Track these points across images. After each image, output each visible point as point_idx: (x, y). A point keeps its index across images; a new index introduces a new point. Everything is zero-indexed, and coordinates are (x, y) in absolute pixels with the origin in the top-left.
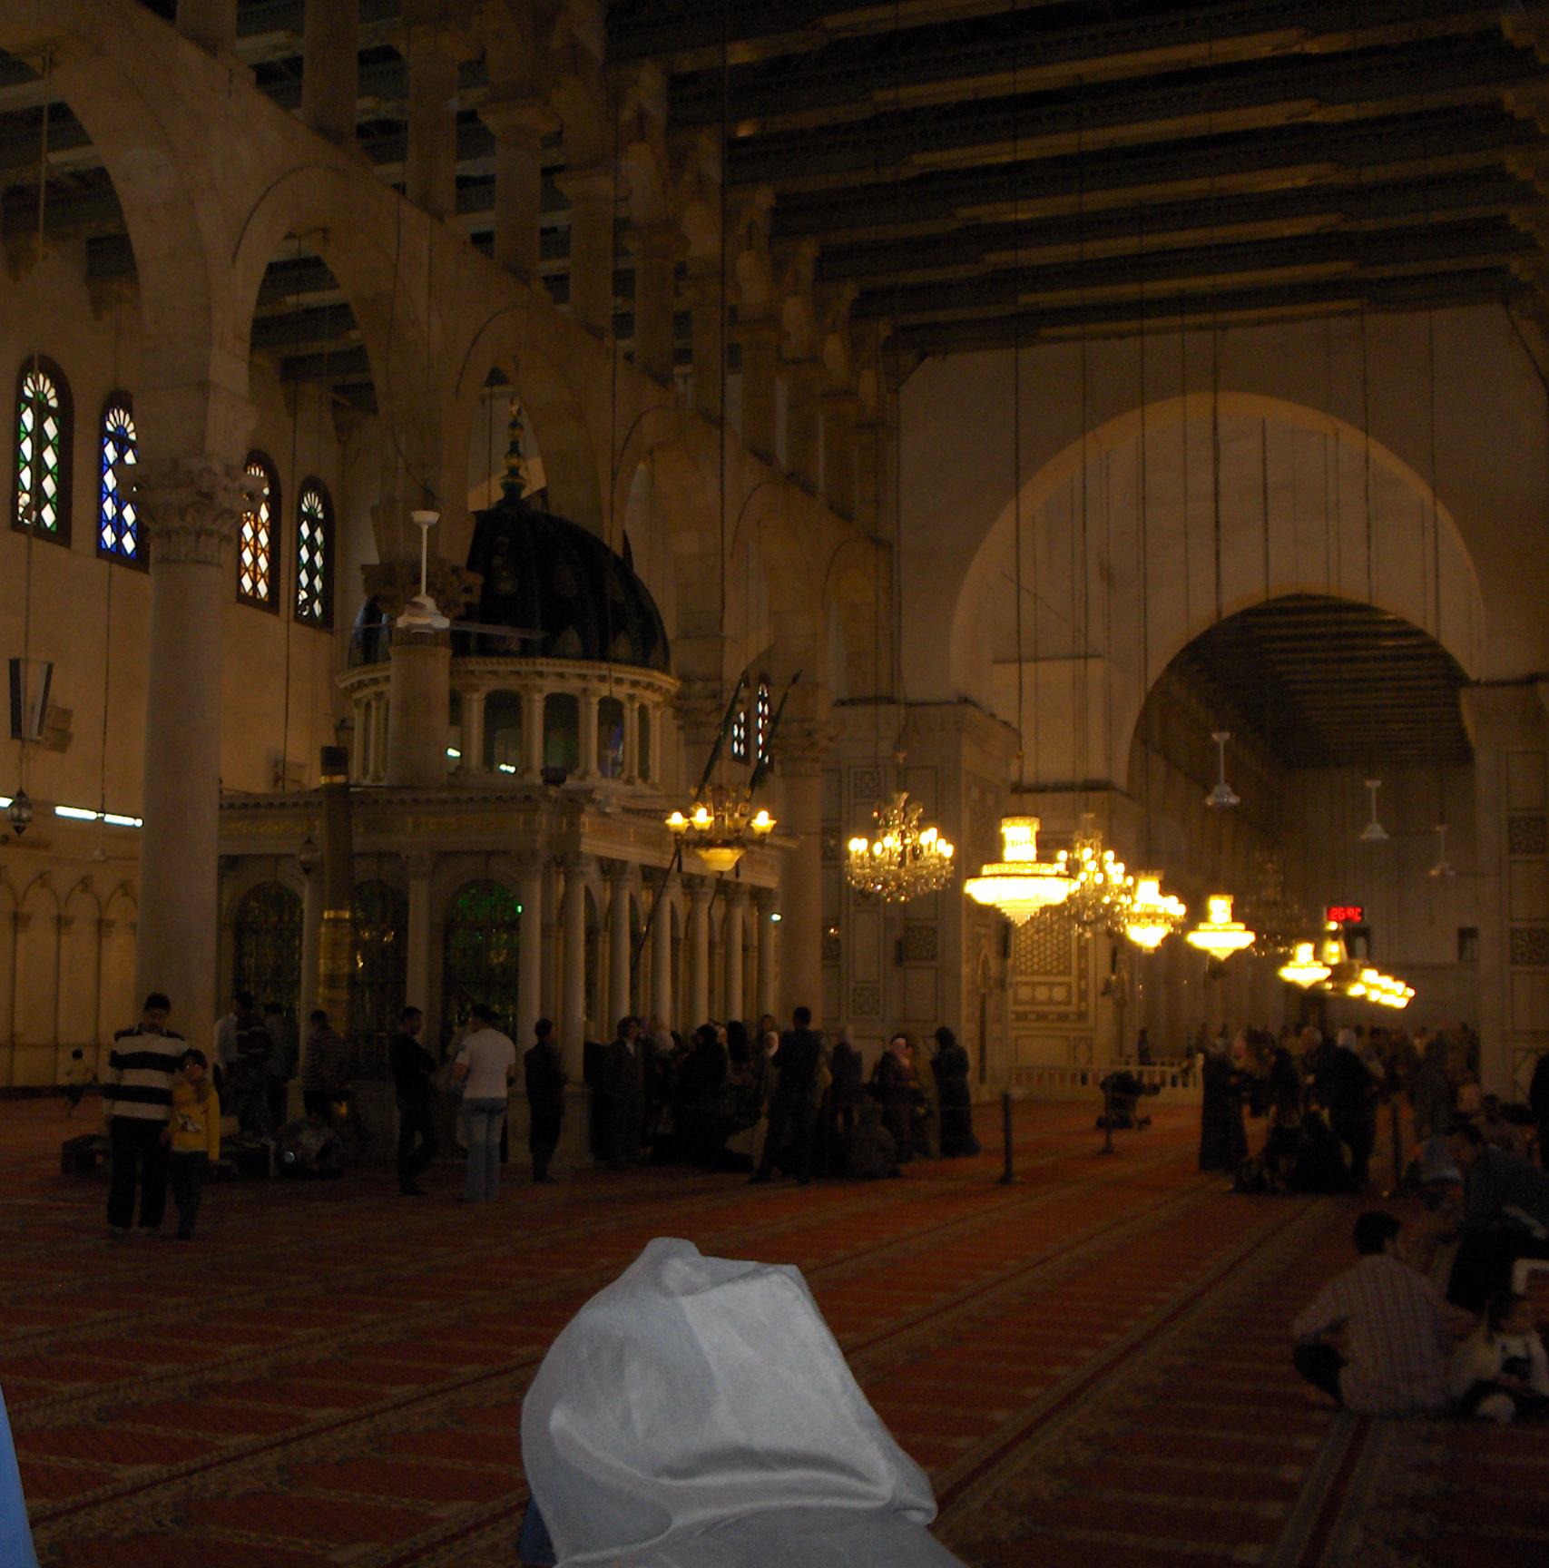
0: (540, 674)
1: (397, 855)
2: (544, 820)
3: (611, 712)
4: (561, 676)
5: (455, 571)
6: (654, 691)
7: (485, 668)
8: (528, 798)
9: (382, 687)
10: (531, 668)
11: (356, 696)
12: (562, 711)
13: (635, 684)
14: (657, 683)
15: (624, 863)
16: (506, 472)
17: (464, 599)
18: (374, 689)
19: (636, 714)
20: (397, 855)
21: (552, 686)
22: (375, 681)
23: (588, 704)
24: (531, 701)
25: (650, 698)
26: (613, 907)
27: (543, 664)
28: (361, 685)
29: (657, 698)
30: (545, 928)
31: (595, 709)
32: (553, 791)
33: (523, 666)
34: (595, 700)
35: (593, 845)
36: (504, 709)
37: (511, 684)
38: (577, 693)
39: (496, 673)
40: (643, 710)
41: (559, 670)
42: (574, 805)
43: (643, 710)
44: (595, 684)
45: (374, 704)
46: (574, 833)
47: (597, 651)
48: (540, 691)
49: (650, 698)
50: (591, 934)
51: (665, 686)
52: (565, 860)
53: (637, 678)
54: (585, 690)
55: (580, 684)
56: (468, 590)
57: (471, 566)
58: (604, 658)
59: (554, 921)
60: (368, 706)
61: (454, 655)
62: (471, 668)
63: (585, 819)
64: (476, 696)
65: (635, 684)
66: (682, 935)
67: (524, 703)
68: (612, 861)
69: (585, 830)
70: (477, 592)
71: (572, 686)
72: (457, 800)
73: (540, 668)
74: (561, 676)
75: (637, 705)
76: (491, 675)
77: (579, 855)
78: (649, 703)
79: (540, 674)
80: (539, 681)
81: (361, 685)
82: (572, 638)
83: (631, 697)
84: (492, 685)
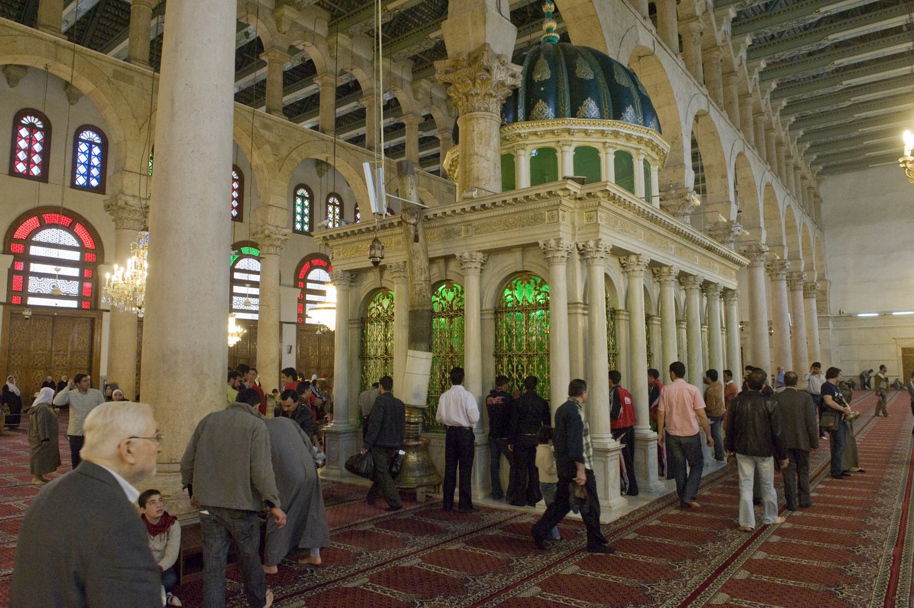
0: (569, 131)
7: (527, 131)
21: (579, 140)
27: (570, 123)
30: (572, 305)
31: (612, 158)
34: (612, 151)
37: (548, 141)
39: (535, 134)
44: (610, 140)
51: (661, 146)
62: (518, 131)
64: (522, 152)
67: (559, 154)
74: (585, 132)
75: (642, 157)
76: (533, 136)
82: (591, 106)
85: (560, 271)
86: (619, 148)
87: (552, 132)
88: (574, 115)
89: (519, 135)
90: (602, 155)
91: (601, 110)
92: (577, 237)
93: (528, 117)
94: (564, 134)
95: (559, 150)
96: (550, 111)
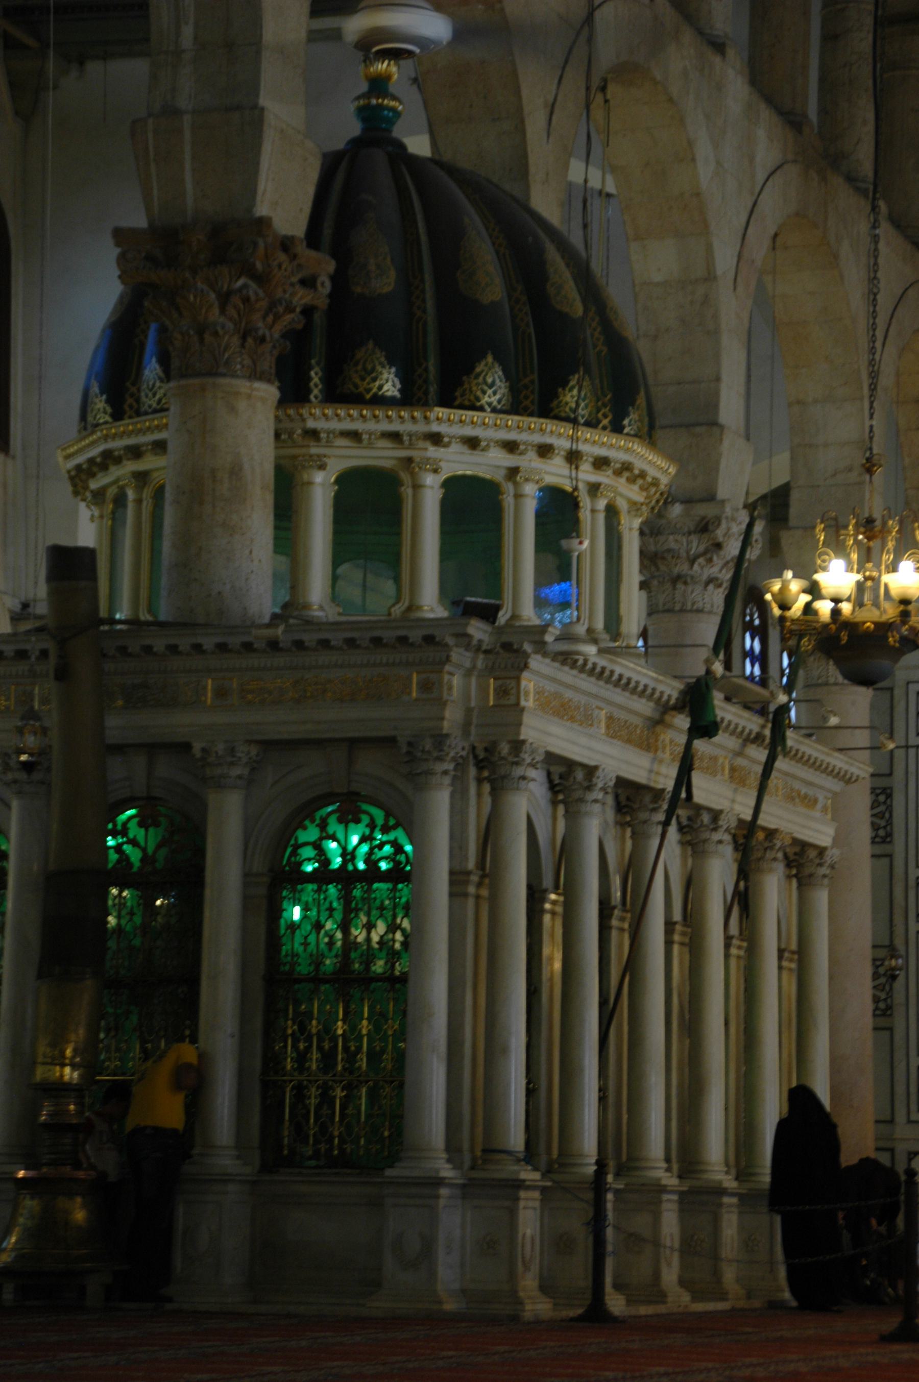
0: (436, 439)
1: (186, 747)
2: (456, 681)
3: (559, 510)
4: (473, 443)
5: (286, 244)
6: (632, 480)
8: (429, 640)
9: (149, 462)
10: (421, 428)
11: (94, 485)
12: (473, 508)
13: (601, 463)
14: (639, 465)
15: (591, 771)
16: (364, 87)
17: (302, 297)
18: (131, 466)
19: (601, 518)
20: (186, 747)
21: (456, 462)
22: (135, 452)
23: (518, 496)
24: (417, 487)
25: (628, 493)
26: (568, 852)
27: (443, 420)
28: (109, 459)
29: (634, 493)
30: (457, 878)
32: (477, 630)
33: (404, 422)
34: (531, 490)
35: (544, 732)
36: (371, 509)
37: (383, 456)
38: (498, 476)
39: (355, 436)
40: (611, 511)
41: (469, 431)
42: (509, 655)
43: (611, 511)
44: (529, 461)
45: (131, 494)
46: (509, 707)
47: (537, 398)
48: (436, 471)
49: (628, 493)
50: (535, 896)
51: (652, 472)
52: (492, 763)
53: (603, 452)
54: (513, 472)
55: (509, 460)
56: (309, 283)
57: (313, 237)
58: (546, 408)
59: (471, 864)
60: (120, 501)
61: (282, 403)
62: (311, 424)
63: (528, 683)
64: (319, 477)
65: (601, 463)
66: (677, 916)
67: (407, 492)
68: (570, 765)
69: (528, 703)
70: (325, 287)
71: (489, 464)
72: (299, 645)
73: (435, 428)
74: (473, 443)
75: (602, 504)
76: (347, 441)
77: (518, 745)
78: (622, 504)
79: (436, 439)
80: (432, 451)
81: (109, 459)
83: (594, 489)
84: (342, 458)
85: (440, 802)
86: (550, 480)
87: (395, 437)
88: (447, 402)
89: (314, 434)
90: (508, 501)
91: (515, 390)
92: (473, 730)
93: (339, 394)
94: (421, 444)
95: (405, 477)
96: (389, 384)
